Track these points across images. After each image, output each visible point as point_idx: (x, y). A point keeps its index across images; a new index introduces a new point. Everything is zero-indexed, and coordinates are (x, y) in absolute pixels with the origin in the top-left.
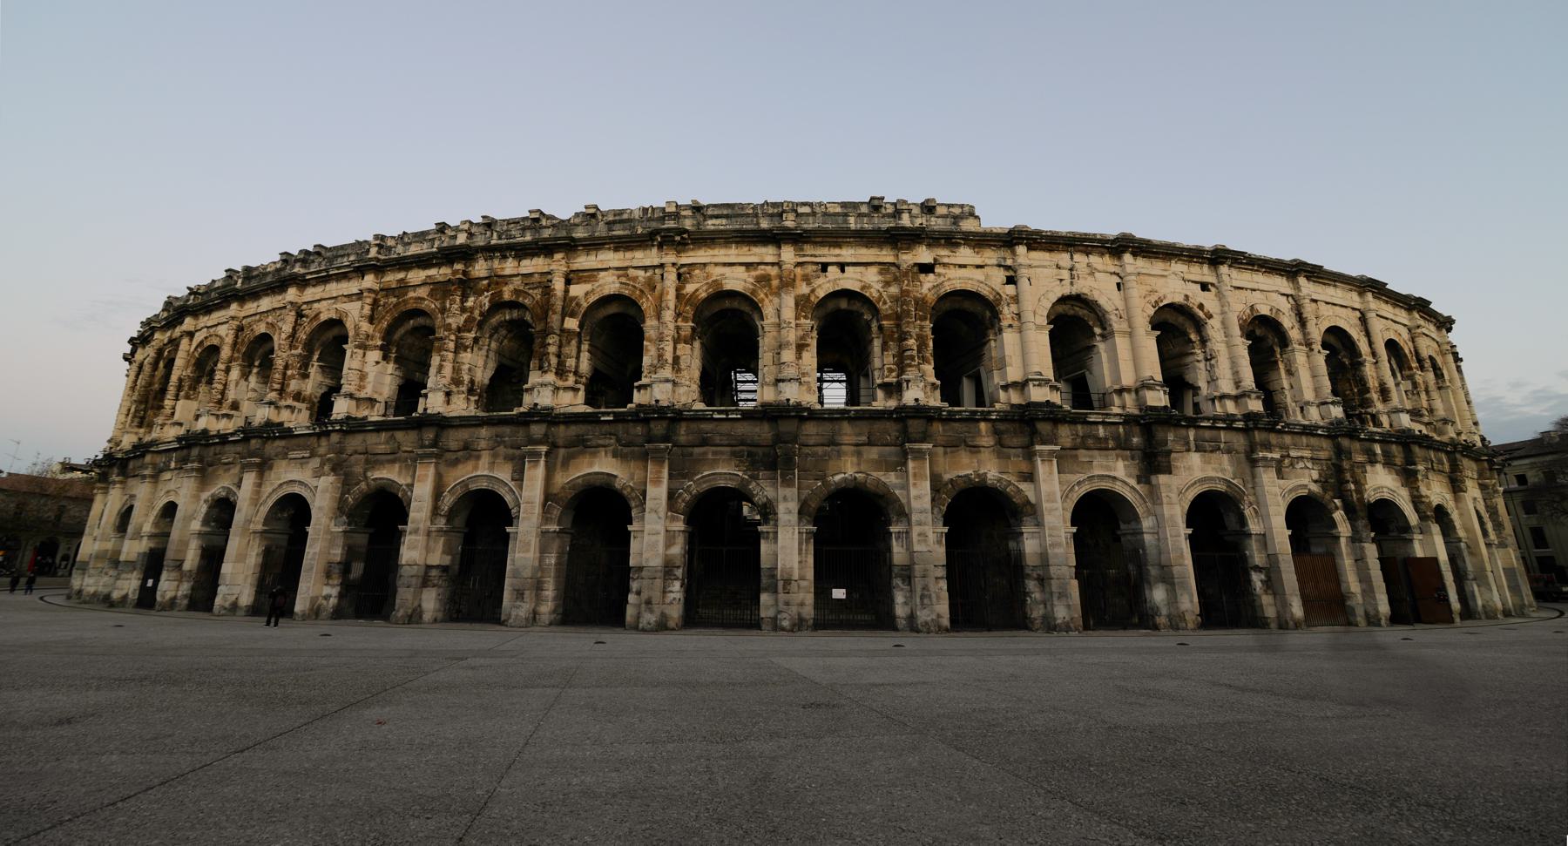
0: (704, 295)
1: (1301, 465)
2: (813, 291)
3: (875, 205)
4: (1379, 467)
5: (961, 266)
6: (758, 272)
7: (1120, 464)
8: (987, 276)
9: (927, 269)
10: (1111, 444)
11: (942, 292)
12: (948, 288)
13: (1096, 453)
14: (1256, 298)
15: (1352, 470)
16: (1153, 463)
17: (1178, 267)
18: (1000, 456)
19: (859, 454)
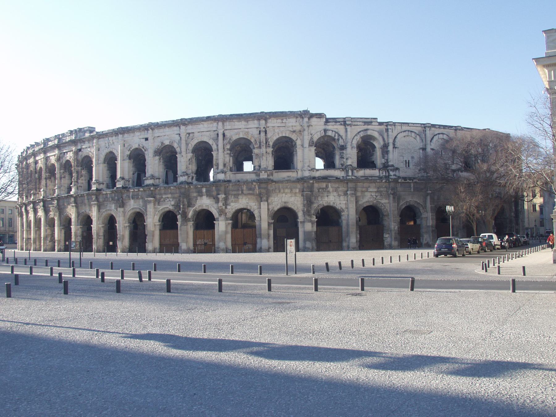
1: (168, 200)
4: (204, 197)
9: (80, 150)
10: (111, 199)
12: (83, 156)
17: (137, 134)
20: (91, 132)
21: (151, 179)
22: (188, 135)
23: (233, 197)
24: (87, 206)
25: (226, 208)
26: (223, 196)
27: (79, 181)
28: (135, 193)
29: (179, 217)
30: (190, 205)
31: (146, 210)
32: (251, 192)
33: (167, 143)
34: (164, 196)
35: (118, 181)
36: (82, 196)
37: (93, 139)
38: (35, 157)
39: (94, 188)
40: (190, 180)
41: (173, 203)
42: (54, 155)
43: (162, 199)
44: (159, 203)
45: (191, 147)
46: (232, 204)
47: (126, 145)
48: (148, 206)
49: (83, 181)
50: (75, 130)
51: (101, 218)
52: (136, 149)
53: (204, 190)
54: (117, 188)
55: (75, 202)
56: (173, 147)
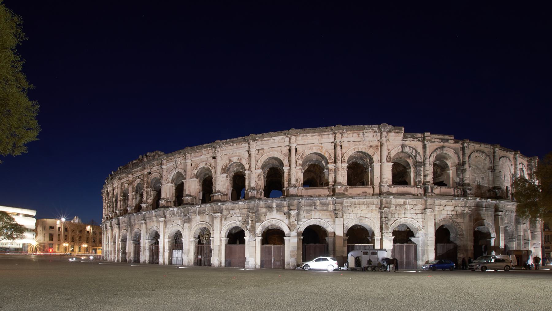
1: (235, 215)
22: (257, 152)
23: (305, 212)
25: (298, 223)
26: (296, 212)
28: (202, 209)
29: (246, 232)
30: (258, 220)
31: (212, 225)
32: (324, 208)
34: (231, 212)
40: (259, 196)
41: (240, 219)
44: (225, 218)
45: (260, 164)
46: (304, 220)
48: (215, 221)
53: (274, 205)
56: (241, 164)
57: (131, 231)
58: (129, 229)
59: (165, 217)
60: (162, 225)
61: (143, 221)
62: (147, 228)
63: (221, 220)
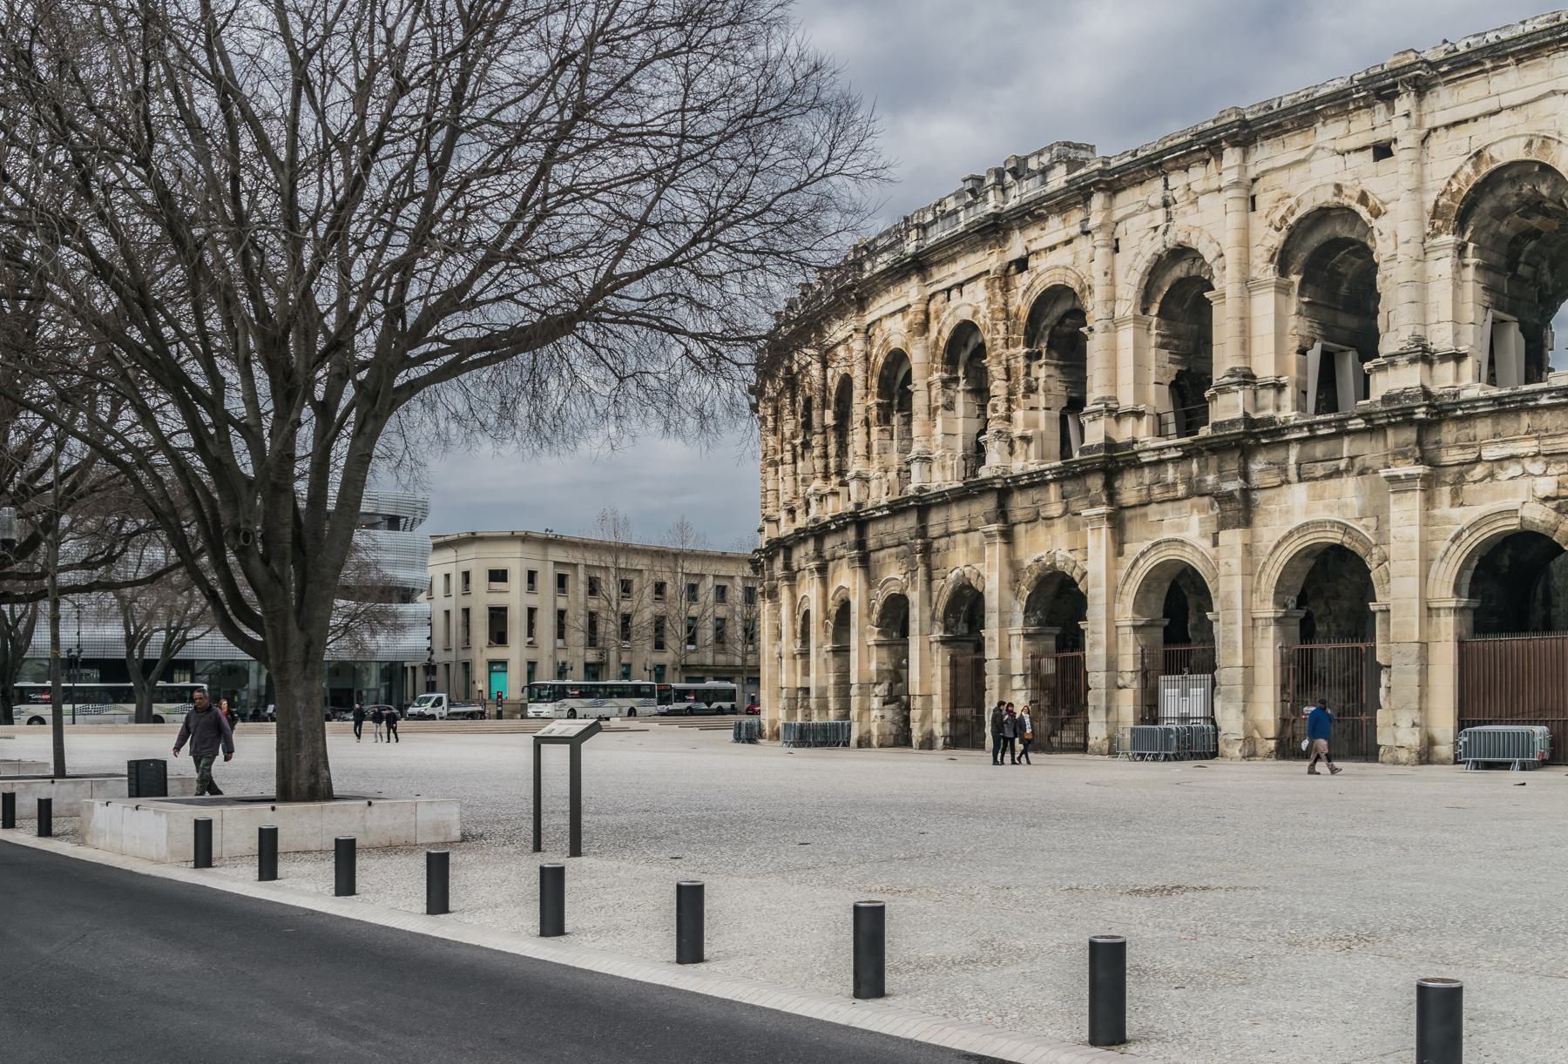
0: (881, 360)
1: (1514, 469)
2: (940, 332)
3: (976, 188)
5: (1052, 248)
6: (911, 317)
7: (1195, 518)
8: (1076, 254)
9: (1022, 264)
10: (1181, 490)
11: (1033, 298)
13: (1168, 506)
14: (1480, 134)
15: (1525, 474)
16: (1240, 510)
17: (1329, 133)
18: (1073, 528)
19: (967, 542)
20: (1073, 165)
21: (1412, 361)
24: (1060, 527)
27: (1019, 415)
33: (1510, 152)
35: (1223, 390)
36: (1036, 482)
37: (1087, 198)
38: (820, 333)
39: (1095, 433)
42: (903, 310)
43: (1479, 471)
47: (1263, 202)
49: (1034, 418)
50: (1000, 174)
51: (1132, 587)
52: (1322, 215)
54: (1216, 426)
55: (1002, 513)
57: (930, 579)
58: (921, 570)
59: (1111, 493)
60: (1098, 540)
61: (994, 527)
62: (1014, 565)
63: (1429, 501)
